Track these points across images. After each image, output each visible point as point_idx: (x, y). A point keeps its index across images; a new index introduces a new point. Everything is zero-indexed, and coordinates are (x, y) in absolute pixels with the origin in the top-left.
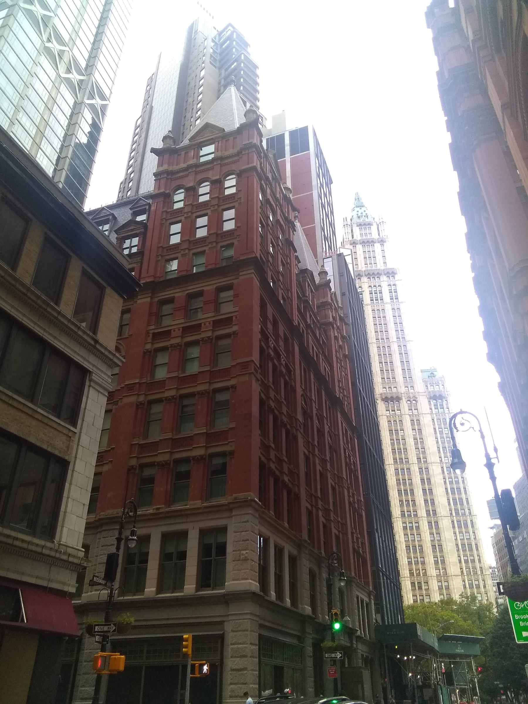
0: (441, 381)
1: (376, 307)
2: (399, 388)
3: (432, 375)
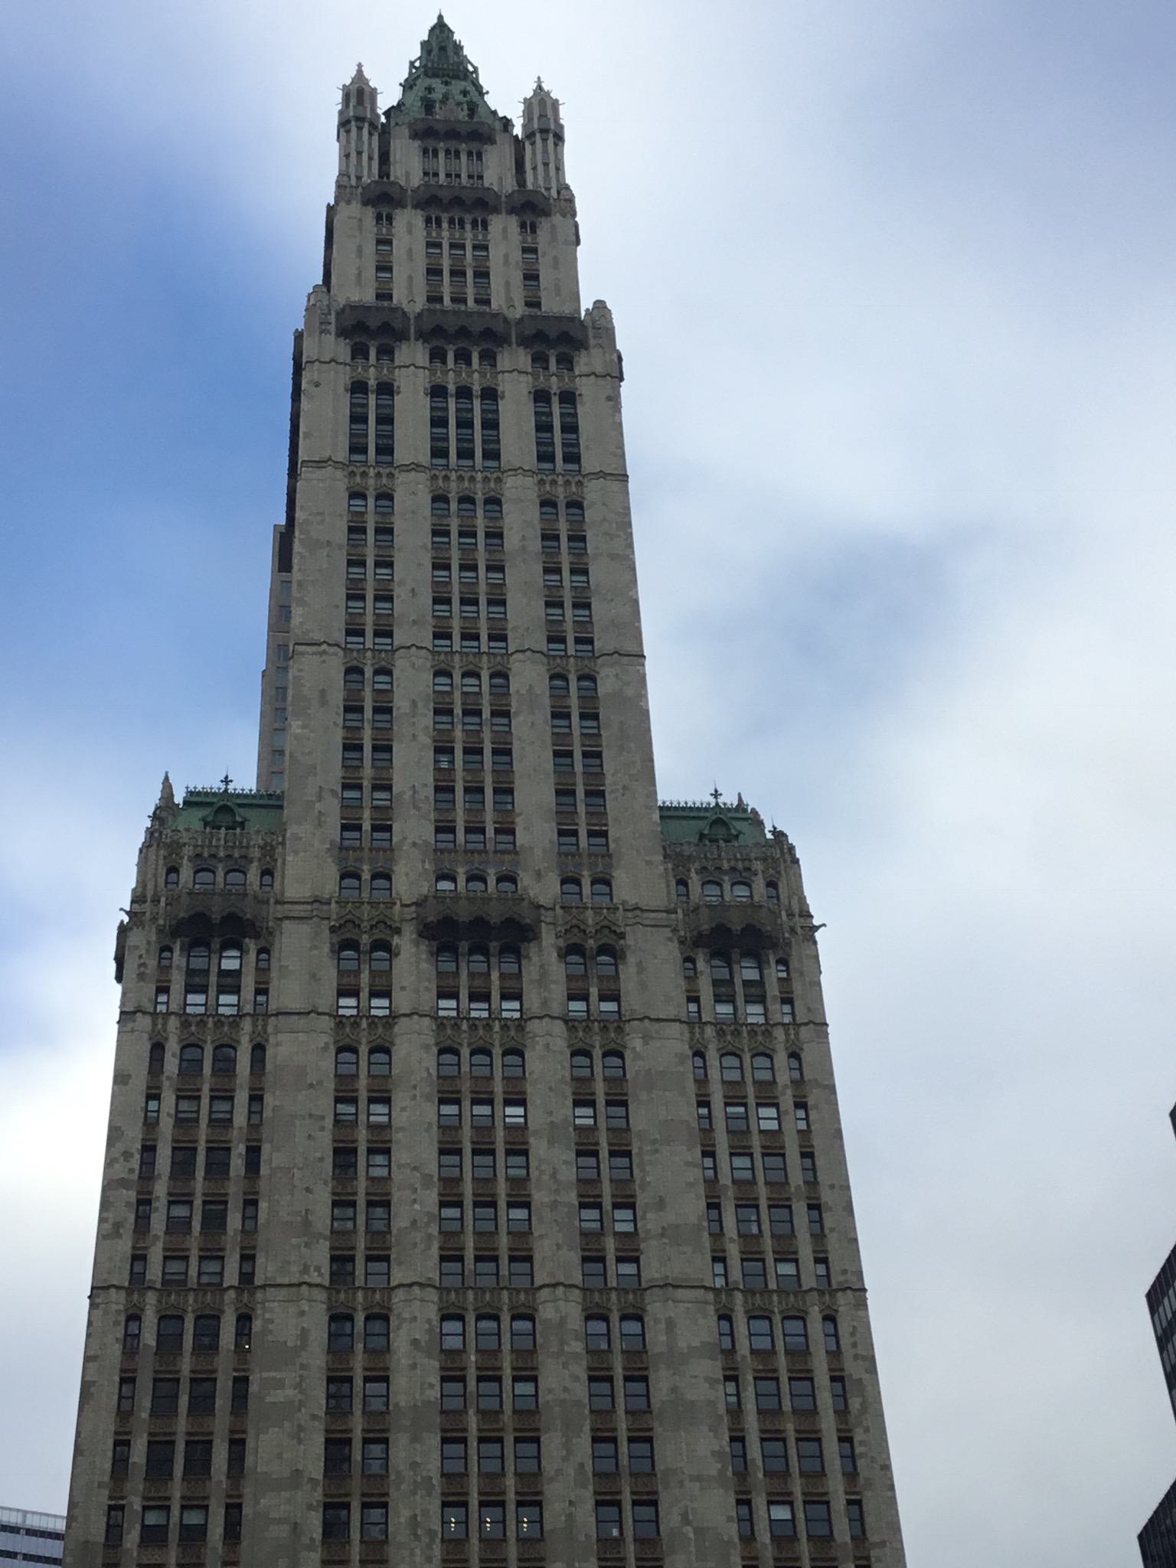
0: (764, 860)
1: (453, 485)
2: (525, 879)
3: (721, 832)
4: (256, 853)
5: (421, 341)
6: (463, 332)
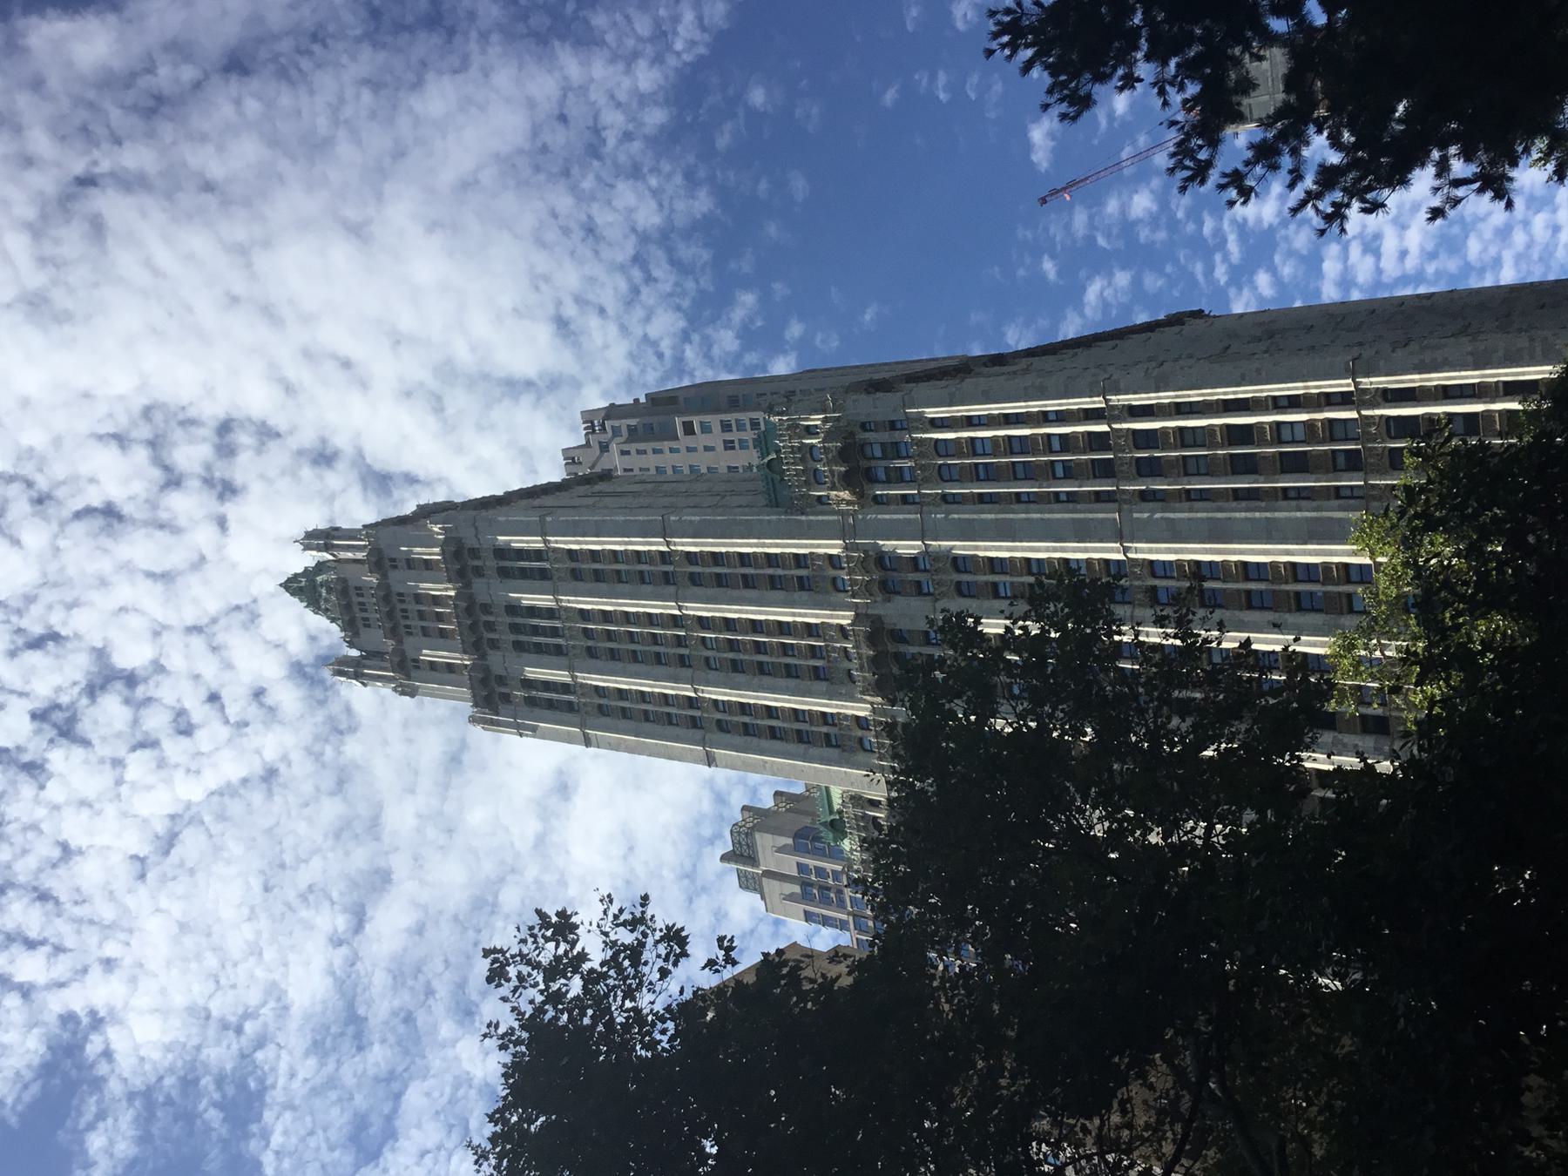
4: (859, 812)
5: (489, 658)
6: (473, 628)
